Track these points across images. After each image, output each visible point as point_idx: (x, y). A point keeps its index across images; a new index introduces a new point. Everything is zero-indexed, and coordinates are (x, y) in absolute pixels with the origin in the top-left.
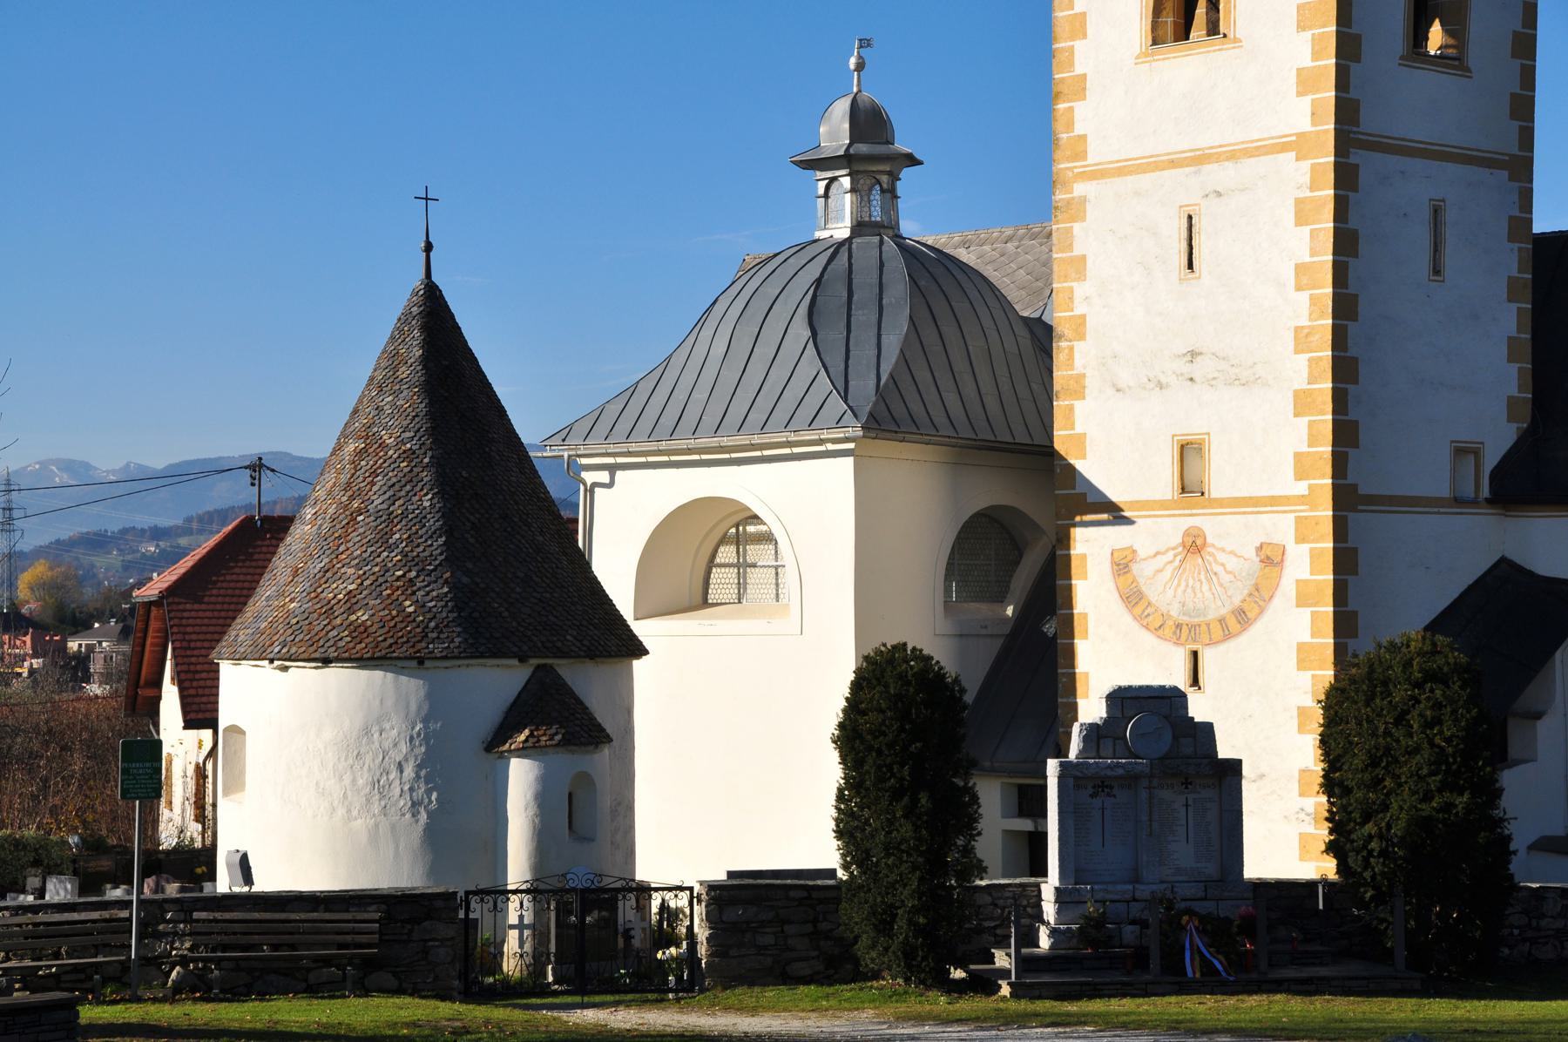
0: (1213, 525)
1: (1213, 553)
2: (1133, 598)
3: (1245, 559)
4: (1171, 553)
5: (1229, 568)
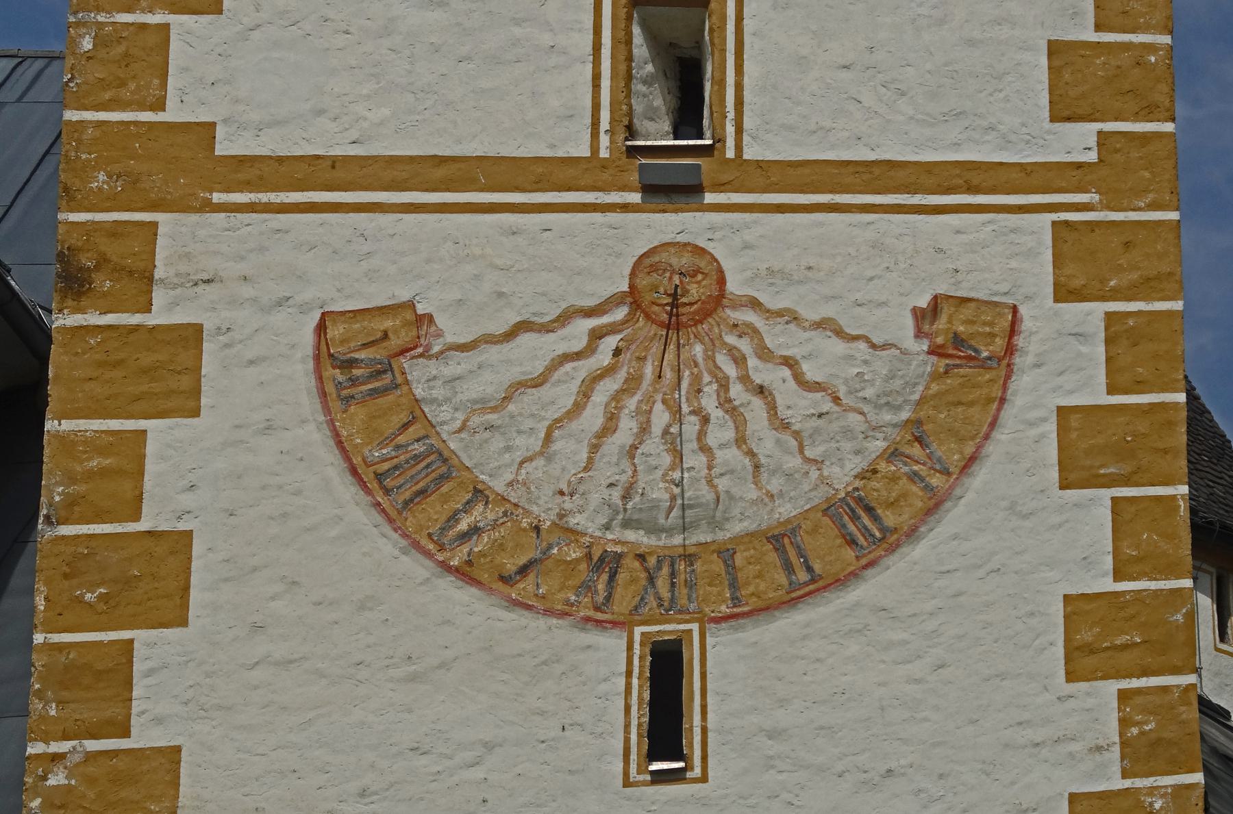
1: (749, 325)
3: (874, 346)
5: (811, 371)
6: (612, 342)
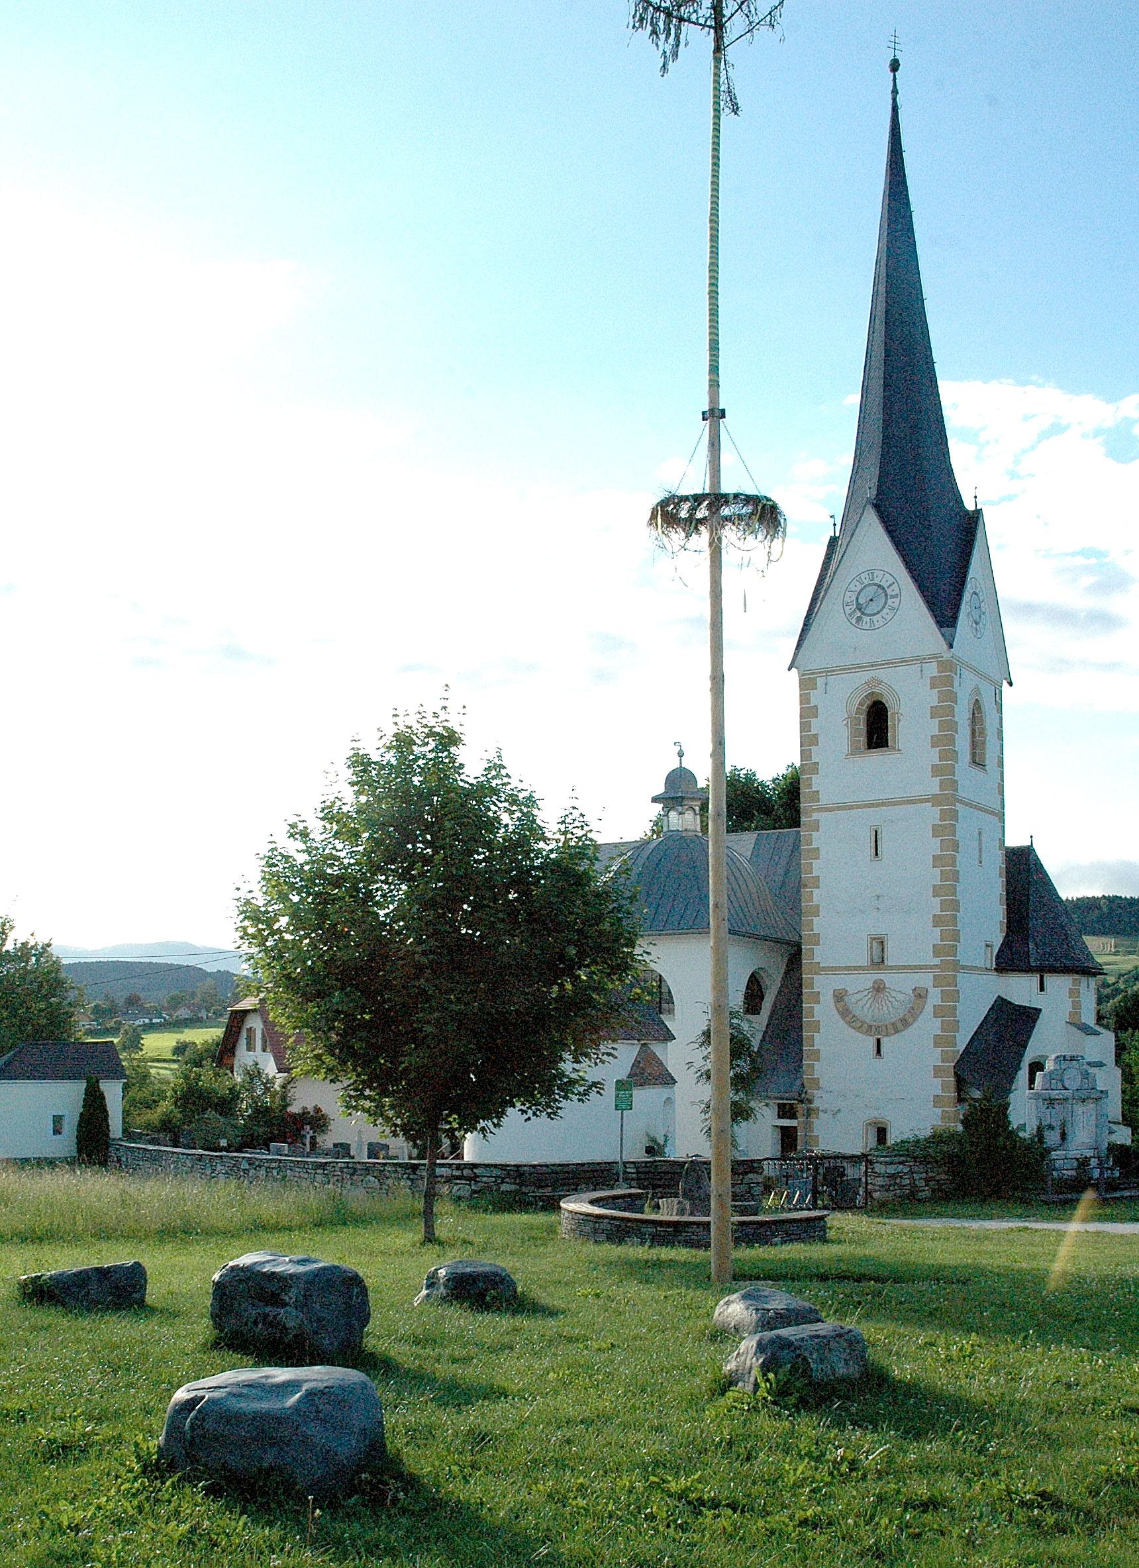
0: (887, 978)
2: (845, 1013)
4: (866, 992)
6: (870, 994)
